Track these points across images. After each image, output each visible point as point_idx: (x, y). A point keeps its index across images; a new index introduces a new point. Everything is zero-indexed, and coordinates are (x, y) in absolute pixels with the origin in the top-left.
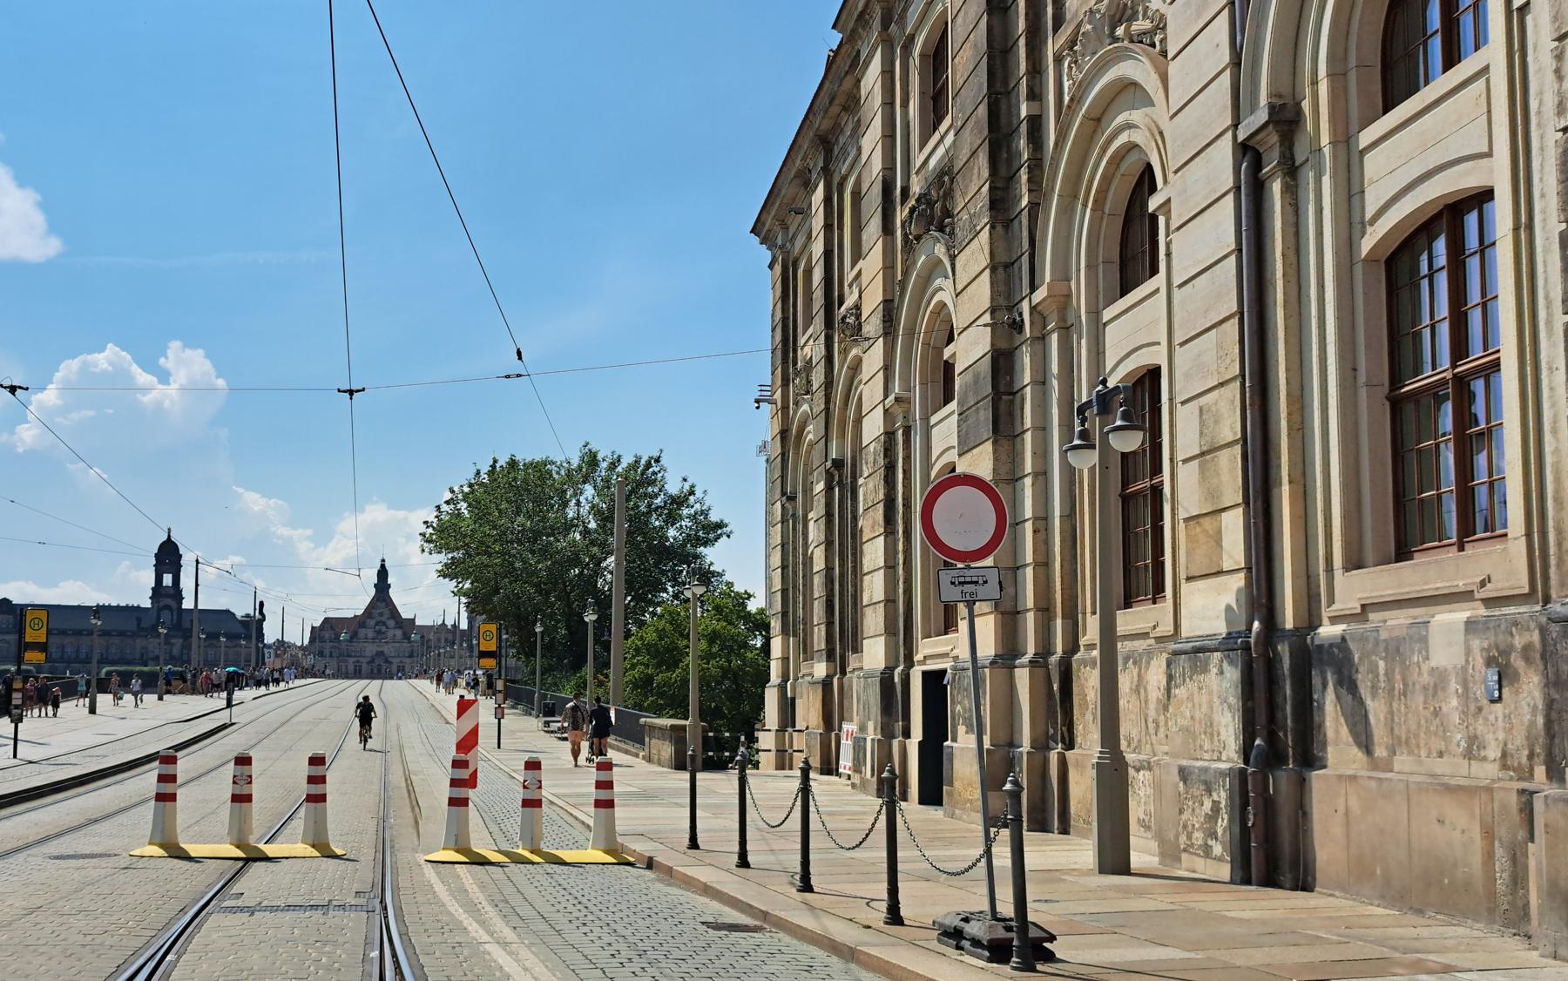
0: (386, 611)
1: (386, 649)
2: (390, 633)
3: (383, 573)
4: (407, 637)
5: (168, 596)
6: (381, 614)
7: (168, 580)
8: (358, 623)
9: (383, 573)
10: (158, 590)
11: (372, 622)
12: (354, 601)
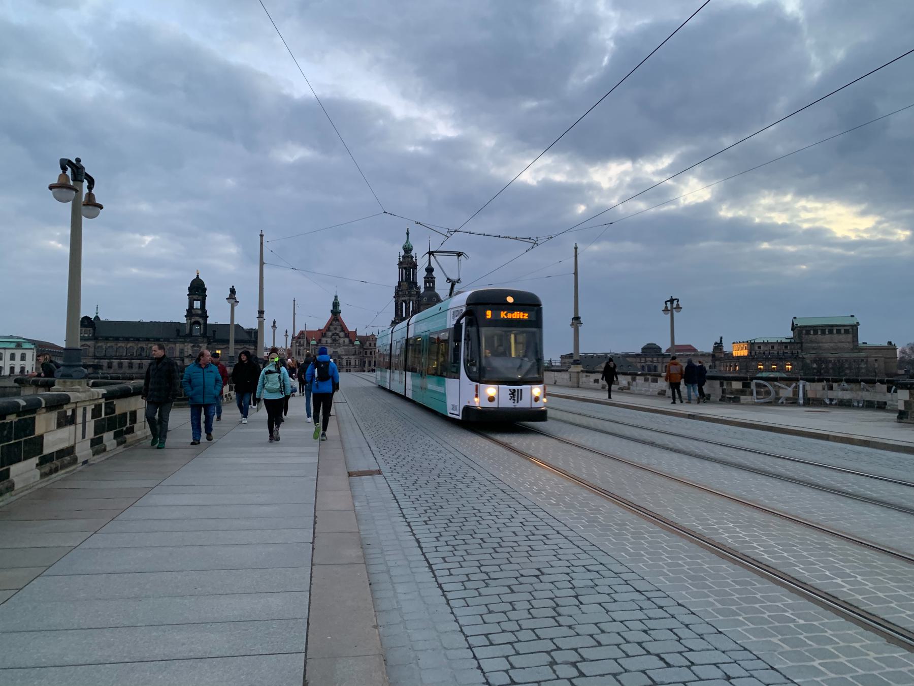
0: (339, 328)
1: (340, 351)
2: (341, 341)
3: (336, 304)
4: (351, 342)
5: (197, 315)
6: (336, 329)
7: (197, 304)
8: (322, 333)
9: (336, 304)
10: (190, 312)
11: (330, 334)
12: (319, 321)
